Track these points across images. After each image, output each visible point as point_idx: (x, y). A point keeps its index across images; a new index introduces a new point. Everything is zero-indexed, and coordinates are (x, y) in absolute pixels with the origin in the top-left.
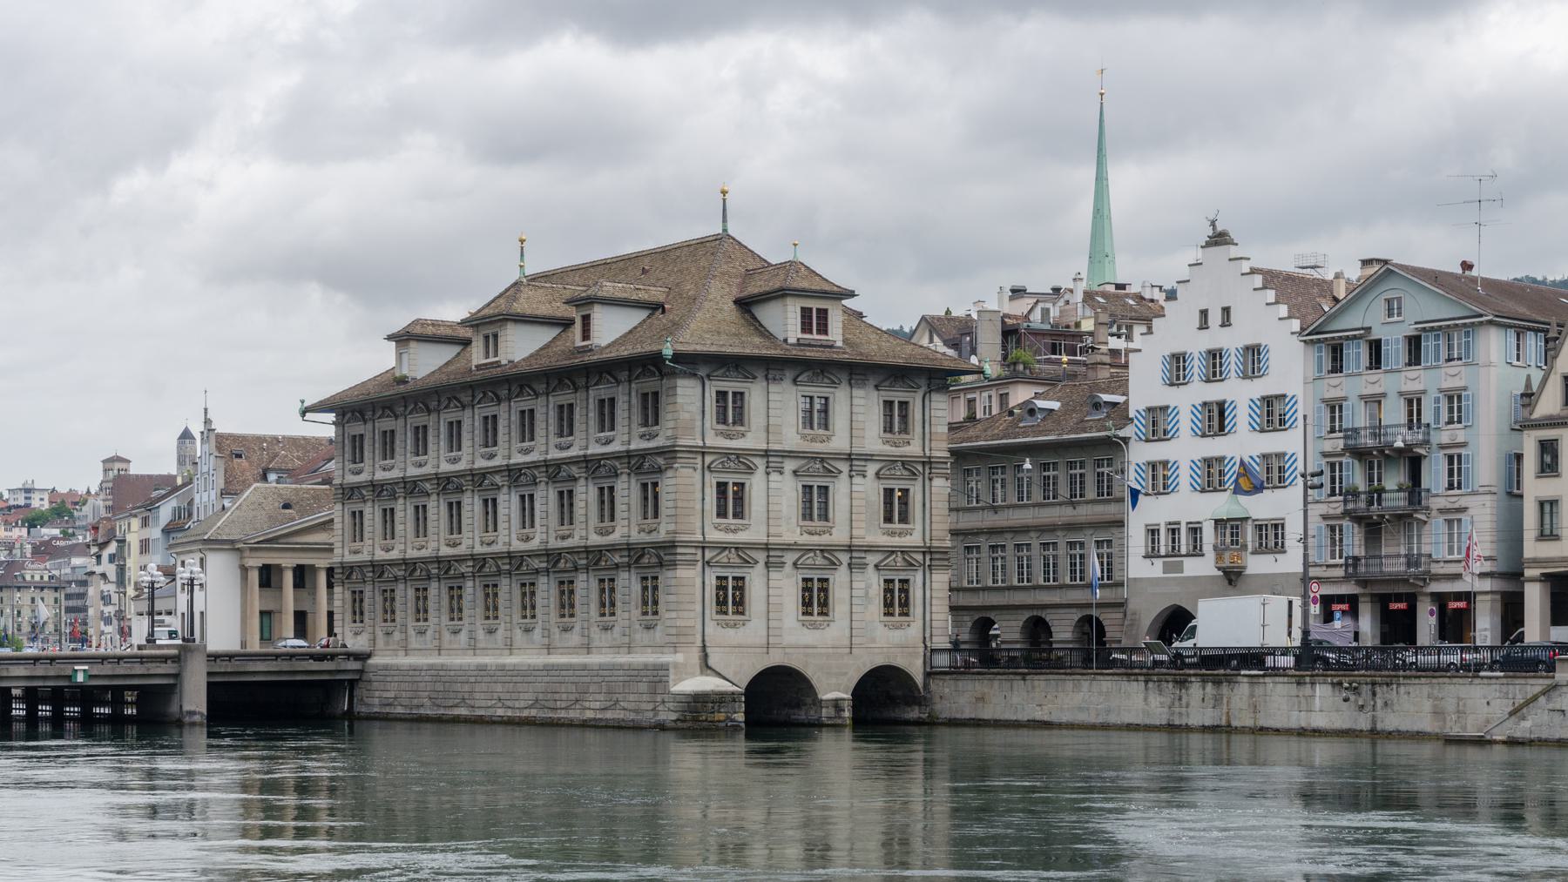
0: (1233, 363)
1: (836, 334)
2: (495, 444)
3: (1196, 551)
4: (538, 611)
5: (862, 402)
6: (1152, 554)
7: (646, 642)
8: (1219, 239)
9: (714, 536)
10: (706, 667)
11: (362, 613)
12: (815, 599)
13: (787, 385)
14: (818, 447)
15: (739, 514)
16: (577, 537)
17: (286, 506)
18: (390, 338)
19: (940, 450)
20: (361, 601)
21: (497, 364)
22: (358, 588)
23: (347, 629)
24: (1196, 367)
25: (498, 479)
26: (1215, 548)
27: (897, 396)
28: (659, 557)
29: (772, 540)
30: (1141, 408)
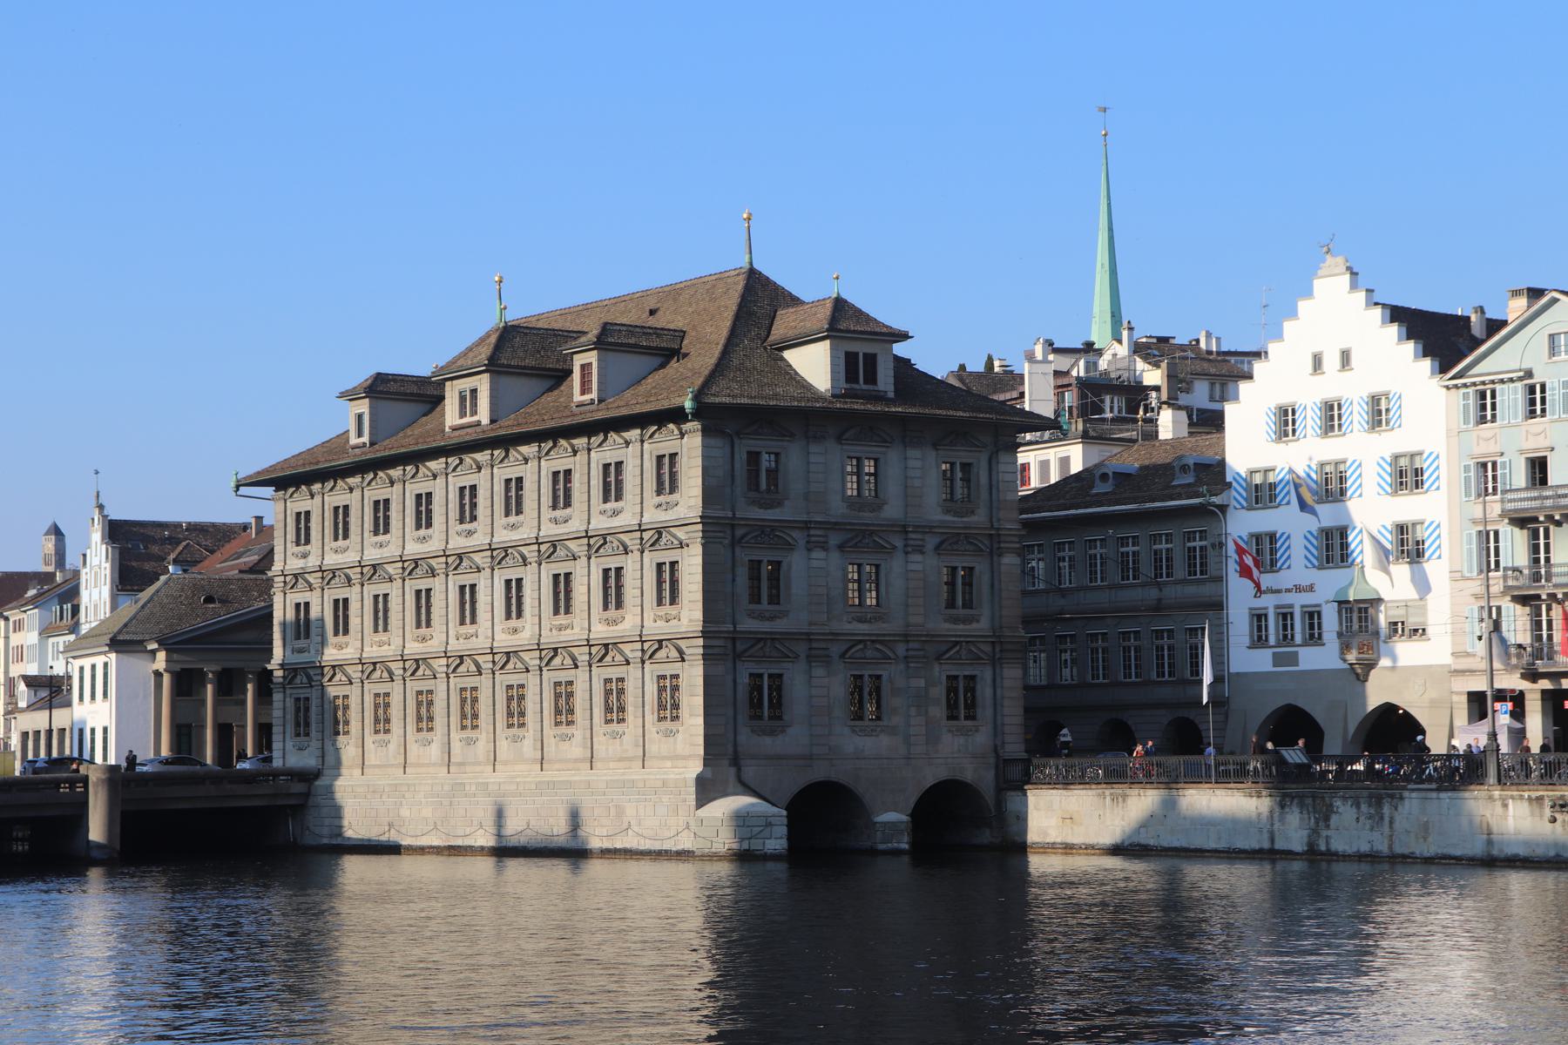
0: (1356, 415)
1: (885, 380)
2: (474, 518)
3: (1314, 637)
5: (918, 464)
6: (1259, 641)
9: (748, 625)
11: (307, 724)
12: (865, 698)
14: (867, 517)
15: (774, 599)
16: (576, 630)
17: (209, 600)
18: (342, 395)
19: (1010, 522)
20: (307, 709)
21: (478, 424)
22: (303, 694)
23: (289, 745)
24: (1310, 420)
25: (477, 558)
26: (1340, 635)
27: (962, 455)
28: (681, 652)
29: (814, 629)
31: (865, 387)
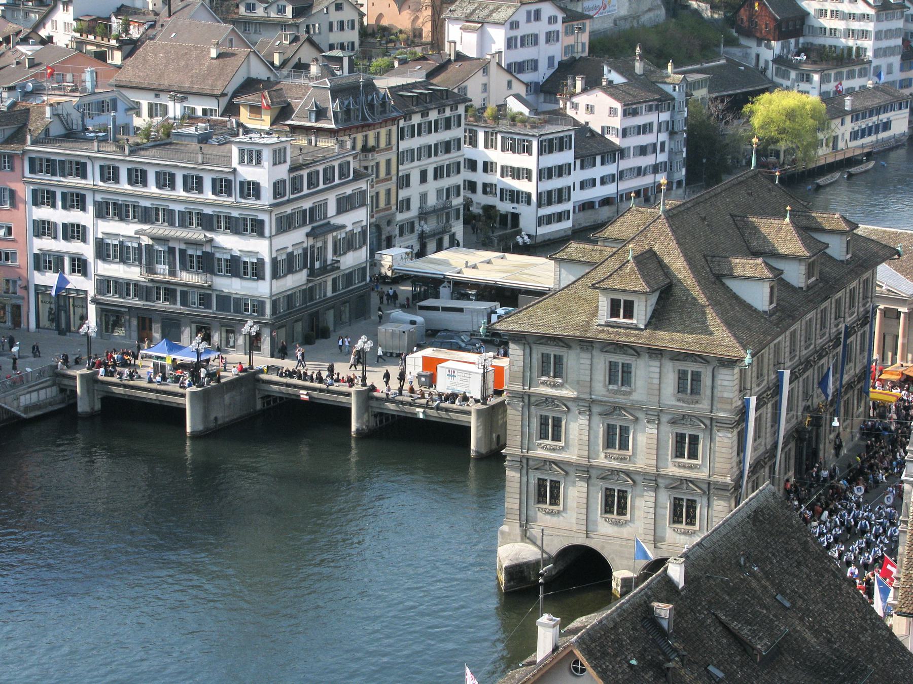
10: (526, 536)
13: (596, 353)
14: (620, 399)
15: (556, 438)
31: (621, 320)
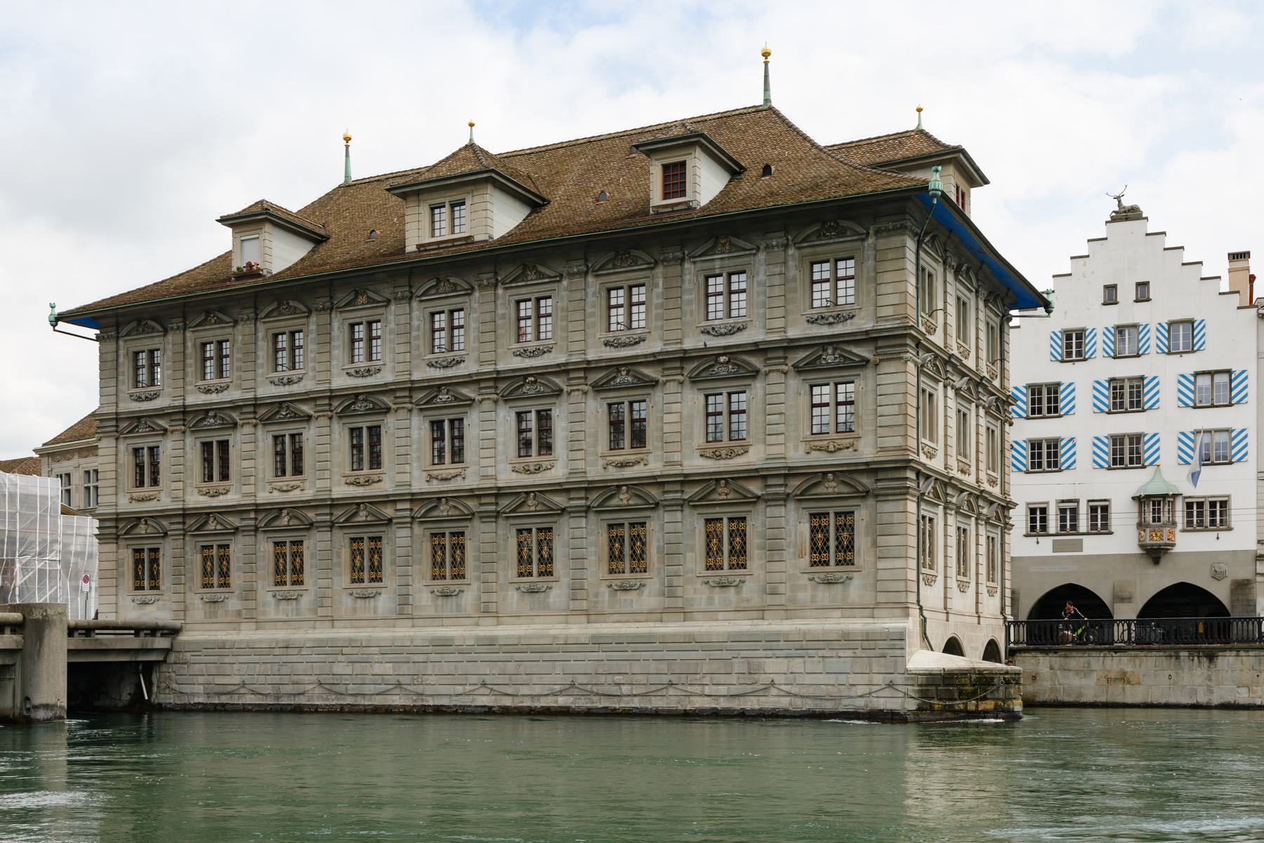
4: (558, 565)
7: (827, 603)
8: (1127, 214)
24: (1098, 344)
30: (1021, 385)
